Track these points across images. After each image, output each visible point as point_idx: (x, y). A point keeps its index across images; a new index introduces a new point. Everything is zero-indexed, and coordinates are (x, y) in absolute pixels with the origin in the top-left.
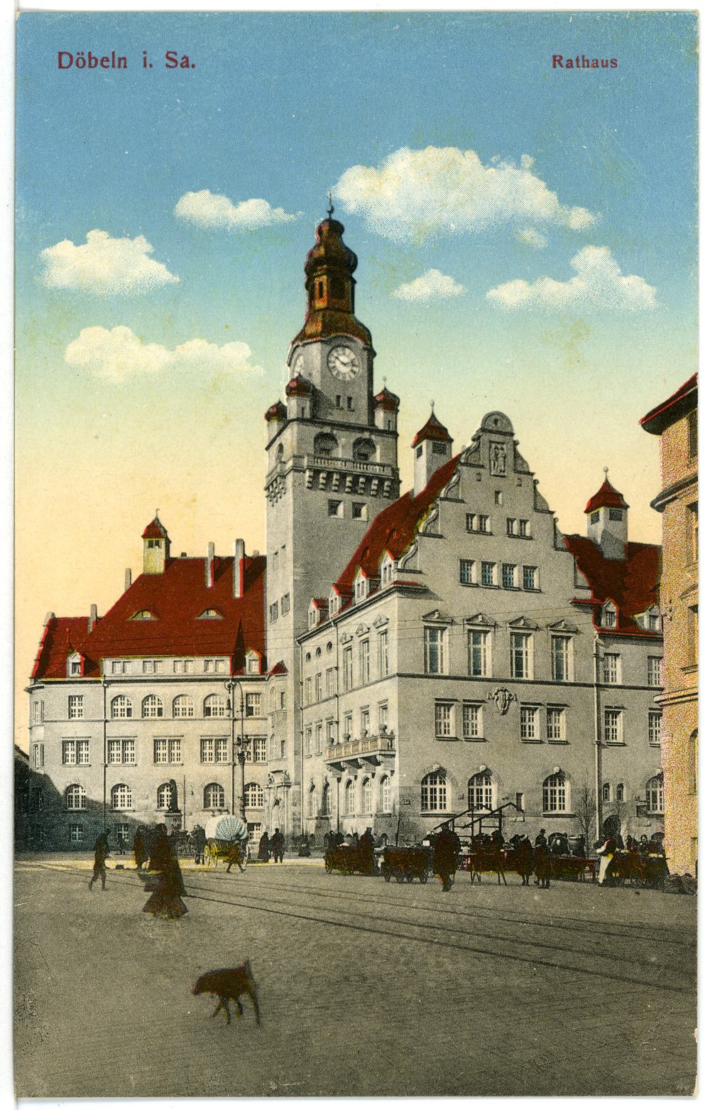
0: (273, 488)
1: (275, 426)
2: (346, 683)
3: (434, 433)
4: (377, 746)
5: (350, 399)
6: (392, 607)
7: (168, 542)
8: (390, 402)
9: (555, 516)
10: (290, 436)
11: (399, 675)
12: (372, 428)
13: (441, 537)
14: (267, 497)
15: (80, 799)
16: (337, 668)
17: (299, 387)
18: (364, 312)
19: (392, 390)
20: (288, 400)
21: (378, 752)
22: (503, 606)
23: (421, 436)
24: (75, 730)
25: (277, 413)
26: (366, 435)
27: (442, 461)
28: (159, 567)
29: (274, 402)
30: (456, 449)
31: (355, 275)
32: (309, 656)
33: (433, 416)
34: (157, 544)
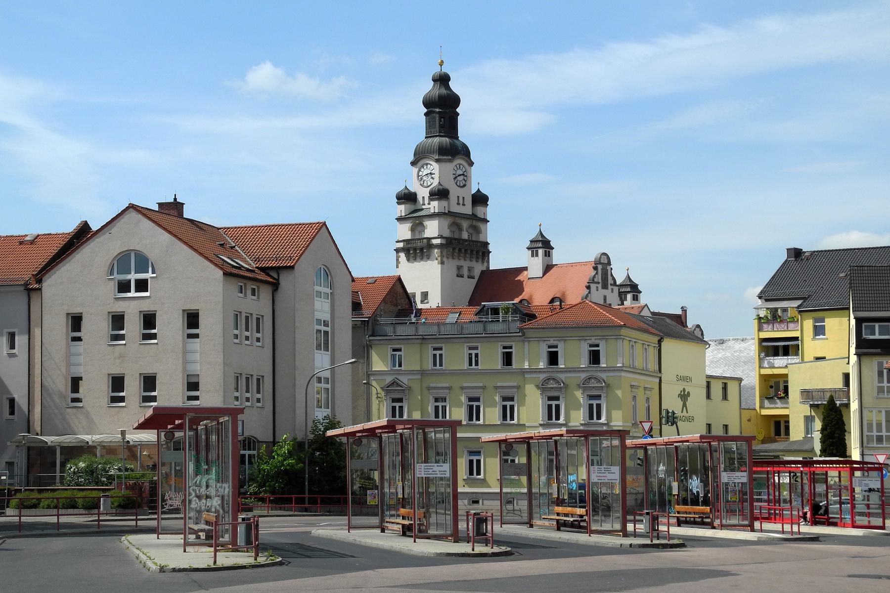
12: (474, 217)
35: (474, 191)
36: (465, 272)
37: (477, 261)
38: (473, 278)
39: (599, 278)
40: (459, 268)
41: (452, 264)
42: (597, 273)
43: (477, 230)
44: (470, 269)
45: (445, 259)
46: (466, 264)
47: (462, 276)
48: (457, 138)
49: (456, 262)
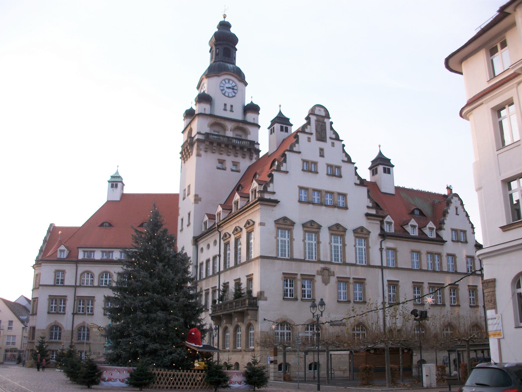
0: (185, 154)
1: (188, 120)
2: (225, 263)
3: (281, 121)
4: (245, 304)
5: (232, 106)
6: (257, 215)
7: (123, 185)
8: (254, 108)
9: (355, 165)
10: (195, 126)
11: (262, 257)
12: (245, 122)
13: (287, 172)
14: (181, 158)
15: (54, 337)
16: (220, 256)
17: (203, 98)
18: (240, 62)
19: (255, 102)
20: (196, 105)
21: (246, 308)
22: (326, 217)
23: (273, 122)
24: (58, 292)
25: (190, 114)
26: (241, 125)
27: (284, 135)
28: (118, 198)
29: (189, 108)
30: (294, 129)
31: (236, 47)
32: (202, 249)
33: (280, 112)
34: (116, 186)
35: (247, 102)
36: (229, 165)
37: (244, 158)
38: (238, 171)
39: (312, 128)
40: (221, 162)
41: (211, 159)
42: (309, 123)
43: (246, 132)
44: (235, 164)
45: (202, 152)
46: (229, 160)
47: (224, 169)
48: (234, 64)
49: (217, 156)
